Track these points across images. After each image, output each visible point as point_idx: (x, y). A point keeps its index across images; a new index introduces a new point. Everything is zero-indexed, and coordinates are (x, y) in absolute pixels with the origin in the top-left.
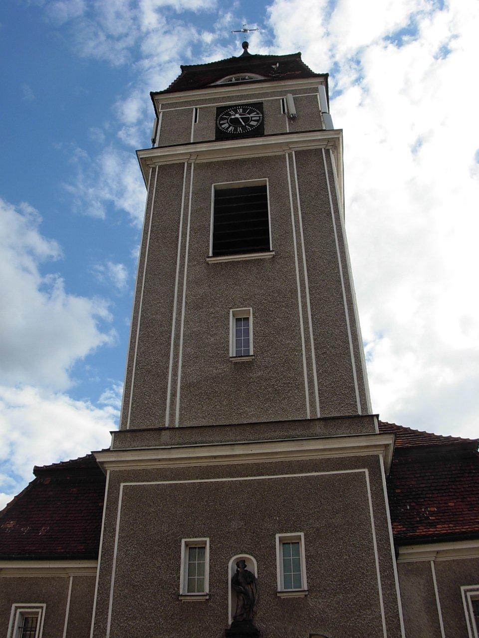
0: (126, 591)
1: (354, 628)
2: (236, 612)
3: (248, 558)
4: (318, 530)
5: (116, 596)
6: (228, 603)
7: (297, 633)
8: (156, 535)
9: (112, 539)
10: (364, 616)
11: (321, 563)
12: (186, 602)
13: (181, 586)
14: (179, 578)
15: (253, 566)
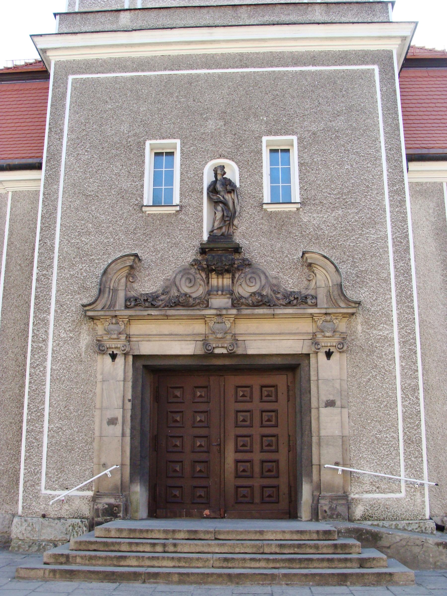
0: (78, 202)
1: (355, 248)
2: (213, 226)
3: (229, 165)
4: (314, 134)
5: (65, 209)
6: (202, 215)
7: (286, 252)
8: (114, 137)
9: (58, 142)
10: (367, 235)
11: (317, 172)
12: (152, 214)
13: (145, 196)
14: (142, 186)
15: (233, 173)
